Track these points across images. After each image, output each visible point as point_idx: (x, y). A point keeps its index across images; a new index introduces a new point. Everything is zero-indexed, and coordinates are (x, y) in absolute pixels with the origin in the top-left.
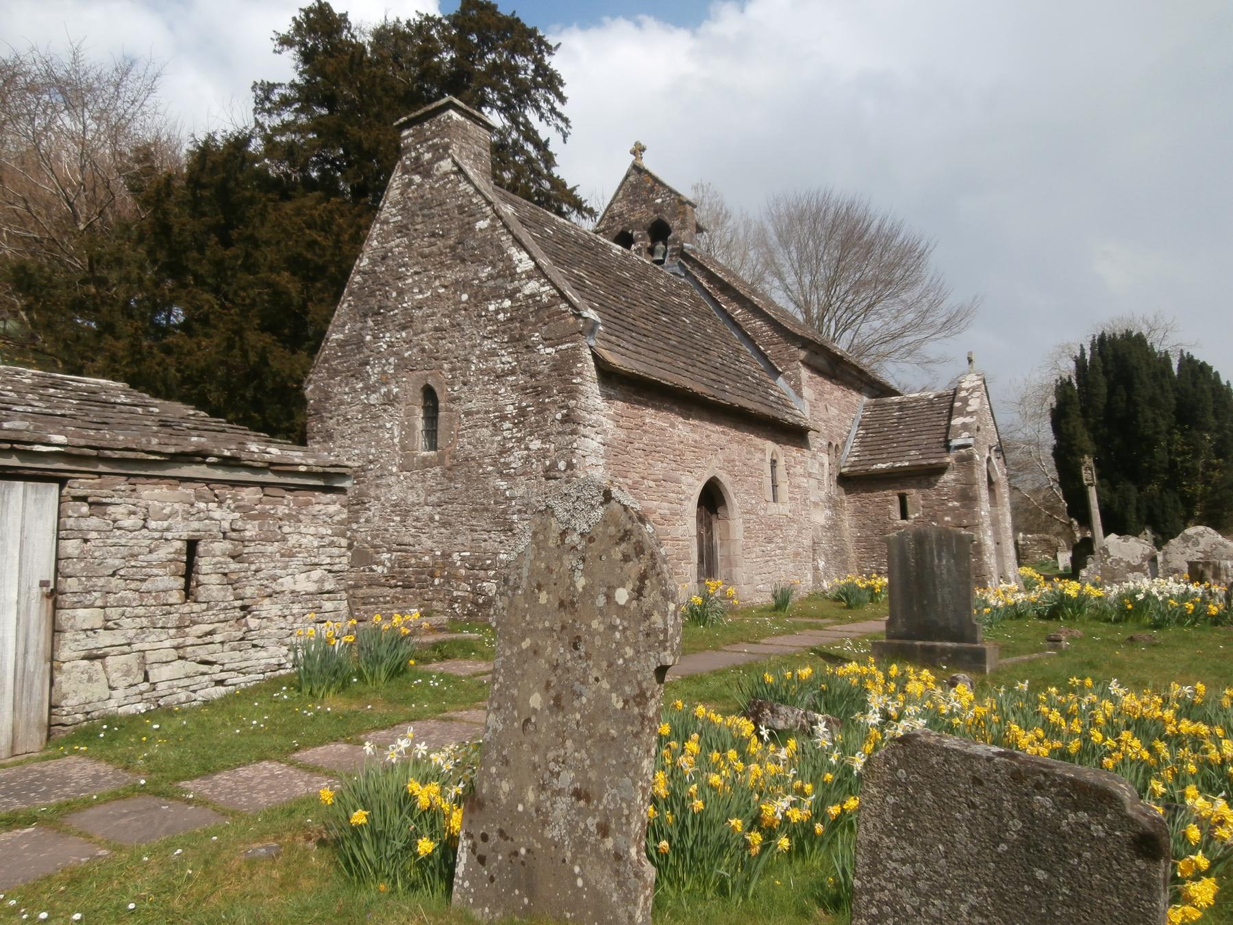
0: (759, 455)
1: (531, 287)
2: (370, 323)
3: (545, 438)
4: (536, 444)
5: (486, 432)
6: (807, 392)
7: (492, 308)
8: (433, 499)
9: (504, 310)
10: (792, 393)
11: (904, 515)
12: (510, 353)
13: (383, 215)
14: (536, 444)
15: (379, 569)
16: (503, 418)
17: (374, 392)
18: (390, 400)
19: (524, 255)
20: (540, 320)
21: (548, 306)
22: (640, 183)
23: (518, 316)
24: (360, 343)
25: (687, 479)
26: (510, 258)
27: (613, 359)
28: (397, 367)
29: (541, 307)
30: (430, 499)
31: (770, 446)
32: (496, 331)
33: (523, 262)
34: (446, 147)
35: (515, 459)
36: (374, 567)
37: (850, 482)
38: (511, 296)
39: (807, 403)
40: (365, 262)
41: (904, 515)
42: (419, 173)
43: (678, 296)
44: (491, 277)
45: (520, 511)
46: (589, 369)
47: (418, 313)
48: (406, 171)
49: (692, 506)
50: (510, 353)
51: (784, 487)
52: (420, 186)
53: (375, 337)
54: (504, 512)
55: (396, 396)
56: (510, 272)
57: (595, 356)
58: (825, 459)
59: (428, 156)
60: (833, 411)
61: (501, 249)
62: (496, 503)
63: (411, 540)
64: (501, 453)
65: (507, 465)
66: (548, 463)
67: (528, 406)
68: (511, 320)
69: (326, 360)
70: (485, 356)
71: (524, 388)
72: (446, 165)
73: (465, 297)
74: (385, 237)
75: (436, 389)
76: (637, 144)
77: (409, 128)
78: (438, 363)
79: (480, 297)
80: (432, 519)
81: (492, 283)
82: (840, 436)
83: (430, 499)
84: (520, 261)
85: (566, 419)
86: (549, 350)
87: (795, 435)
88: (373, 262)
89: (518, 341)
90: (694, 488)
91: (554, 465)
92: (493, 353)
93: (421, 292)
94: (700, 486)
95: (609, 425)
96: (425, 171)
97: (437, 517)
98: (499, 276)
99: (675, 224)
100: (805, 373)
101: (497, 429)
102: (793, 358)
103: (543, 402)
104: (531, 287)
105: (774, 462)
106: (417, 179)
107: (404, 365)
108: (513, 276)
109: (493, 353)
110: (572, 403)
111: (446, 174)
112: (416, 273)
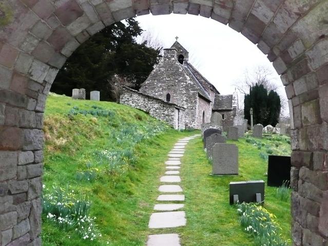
1: (190, 82)
4: (189, 105)
5: (180, 102)
14: (189, 105)
22: (177, 46)
29: (191, 85)
34: (174, 56)
46: (197, 95)
57: (199, 93)
61: (184, 75)
75: (171, 95)
79: (180, 81)
87: (209, 101)
89: (187, 90)
104: (190, 82)
106: (167, 59)
108: (186, 80)
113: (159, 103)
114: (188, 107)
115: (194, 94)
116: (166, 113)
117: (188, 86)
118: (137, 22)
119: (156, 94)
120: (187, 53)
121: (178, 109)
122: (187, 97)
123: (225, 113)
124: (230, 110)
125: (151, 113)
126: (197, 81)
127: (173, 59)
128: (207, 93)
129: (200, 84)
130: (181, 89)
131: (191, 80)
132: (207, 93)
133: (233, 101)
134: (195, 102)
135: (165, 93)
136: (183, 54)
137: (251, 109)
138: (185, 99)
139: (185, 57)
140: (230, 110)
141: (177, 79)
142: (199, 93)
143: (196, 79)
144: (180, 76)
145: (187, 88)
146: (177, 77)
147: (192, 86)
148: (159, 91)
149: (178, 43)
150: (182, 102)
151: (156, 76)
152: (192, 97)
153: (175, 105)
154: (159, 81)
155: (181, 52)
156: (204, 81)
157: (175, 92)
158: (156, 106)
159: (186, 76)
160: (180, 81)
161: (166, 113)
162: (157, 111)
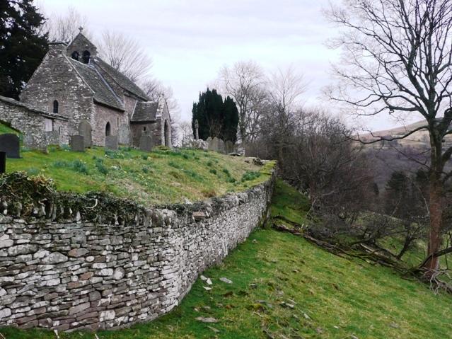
6: (125, 102)
13: (44, 61)
22: (81, 39)
27: (98, 100)
33: (80, 81)
35: (77, 117)
37: (131, 123)
40: (38, 71)
49: (105, 127)
56: (77, 81)
57: (94, 99)
58: (127, 117)
61: (75, 76)
72: (61, 56)
79: (69, 84)
89: (79, 95)
96: (56, 55)
100: (124, 97)
104: (82, 85)
108: (78, 82)
113: (22, 111)
115: (87, 100)
116: (32, 123)
117: (80, 91)
118: (34, 7)
119: (41, 101)
120: (93, 48)
121: (52, 119)
122: (79, 104)
123: (147, 126)
124: (154, 122)
125: (13, 124)
126: (107, 84)
128: (119, 100)
129: (110, 89)
131: (83, 82)
132: (119, 100)
133: (158, 110)
134: (90, 111)
135: (52, 99)
136: (89, 50)
139: (91, 53)
140: (154, 122)
141: (66, 82)
142: (94, 99)
143: (105, 82)
144: (70, 78)
145: (79, 92)
146: (66, 79)
147: (85, 91)
148: (44, 97)
149: (82, 36)
150: (73, 110)
151: (40, 79)
152: (84, 105)
153: (43, 113)
154: (44, 84)
155: (86, 47)
157: (64, 98)
158: (20, 114)
159: (77, 77)
160: (69, 84)
161: (32, 123)
162: (21, 121)
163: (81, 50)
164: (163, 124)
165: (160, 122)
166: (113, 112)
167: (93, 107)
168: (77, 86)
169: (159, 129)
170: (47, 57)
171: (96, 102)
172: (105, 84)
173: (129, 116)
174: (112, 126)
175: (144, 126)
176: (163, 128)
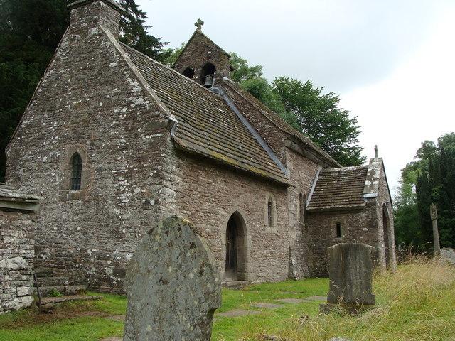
0: (262, 200)
2: (46, 116)
3: (143, 186)
4: (137, 190)
6: (289, 164)
7: (116, 111)
8: (76, 218)
9: (123, 113)
10: (281, 164)
11: (339, 235)
12: (126, 137)
15: (44, 257)
16: (119, 174)
17: (45, 155)
18: (55, 161)
19: (136, 83)
20: (144, 120)
21: (149, 112)
22: (199, 42)
23: (131, 117)
24: (40, 127)
25: (222, 212)
26: (128, 84)
27: (184, 143)
28: (59, 142)
30: (74, 218)
31: (268, 195)
32: (117, 125)
34: (96, 20)
35: (124, 197)
36: (42, 255)
37: (308, 215)
38: (128, 104)
39: (289, 171)
41: (339, 235)
42: (79, 34)
43: (219, 107)
44: (116, 94)
45: (127, 227)
47: (73, 112)
48: (72, 32)
49: (223, 228)
50: (126, 137)
51: (275, 217)
52: (79, 41)
53: (49, 124)
54: (117, 228)
55: (58, 158)
57: (173, 141)
58: (297, 201)
59: (85, 25)
60: (303, 175)
62: (113, 222)
63: (63, 241)
64: (117, 194)
65: (121, 200)
66: (144, 201)
67: (133, 168)
68: (126, 119)
69: (20, 135)
70: (110, 139)
71: (133, 158)
72: (95, 30)
73: (101, 104)
74: (56, 68)
75: (82, 156)
76: (199, 20)
77: (75, 8)
78: (84, 140)
79: (109, 105)
80: (76, 230)
81: (117, 97)
82: (307, 189)
83: (74, 218)
84: (134, 86)
85: (156, 176)
86: (147, 137)
87: (281, 188)
88: (50, 81)
89: (131, 132)
90: (225, 216)
91: (148, 202)
92: (116, 137)
93: (76, 100)
94: (228, 216)
95: (179, 180)
96: (83, 33)
97: (79, 229)
98: (121, 93)
99: (218, 66)
100: (288, 154)
101: (116, 179)
102: (282, 144)
103: (143, 166)
104: (139, 101)
105: (270, 204)
106: (78, 37)
107: (64, 141)
108: (129, 94)
109: (116, 137)
110: (159, 167)
111: (95, 35)
112: (74, 89)
114: (132, 199)
115: (153, 146)
117: (134, 119)
119: (45, 159)
123: (343, 220)
124: (359, 210)
126: (249, 127)
127: (95, 30)
128: (277, 161)
129: (256, 137)
130: (112, 132)
133: (368, 183)
135: (66, 152)
137: (433, 206)
138: (123, 170)
140: (359, 210)
141: (103, 98)
143: (246, 123)
144: (111, 84)
150: (116, 179)
155: (209, 57)
156: (267, 126)
159: (130, 80)
163: (198, 64)
164: (379, 214)
165: (374, 212)
166: (253, 186)
167: (172, 166)
168: (128, 104)
169: (372, 225)
170: (65, 43)
171: (180, 152)
172: (244, 127)
173: (302, 197)
174: (250, 224)
175: (337, 219)
176: (380, 224)
